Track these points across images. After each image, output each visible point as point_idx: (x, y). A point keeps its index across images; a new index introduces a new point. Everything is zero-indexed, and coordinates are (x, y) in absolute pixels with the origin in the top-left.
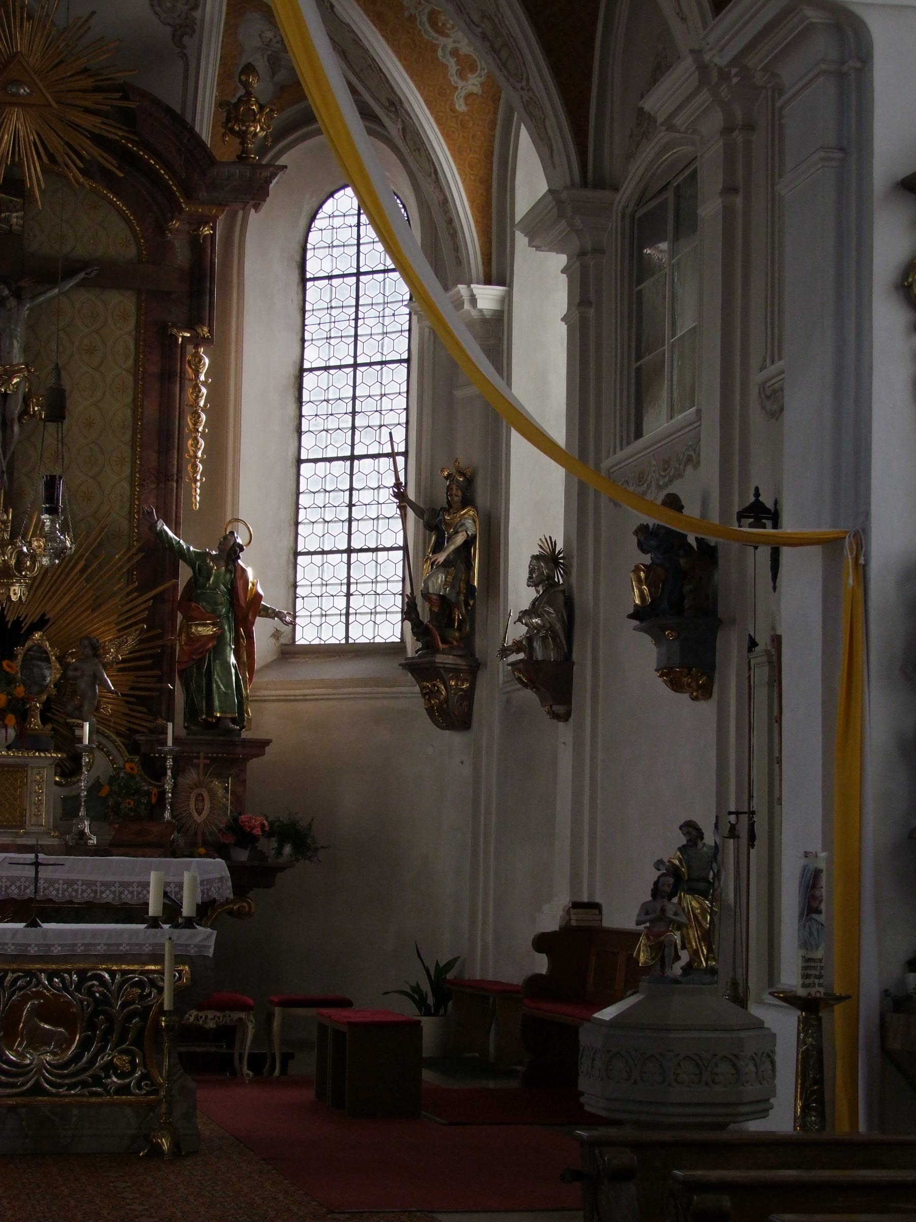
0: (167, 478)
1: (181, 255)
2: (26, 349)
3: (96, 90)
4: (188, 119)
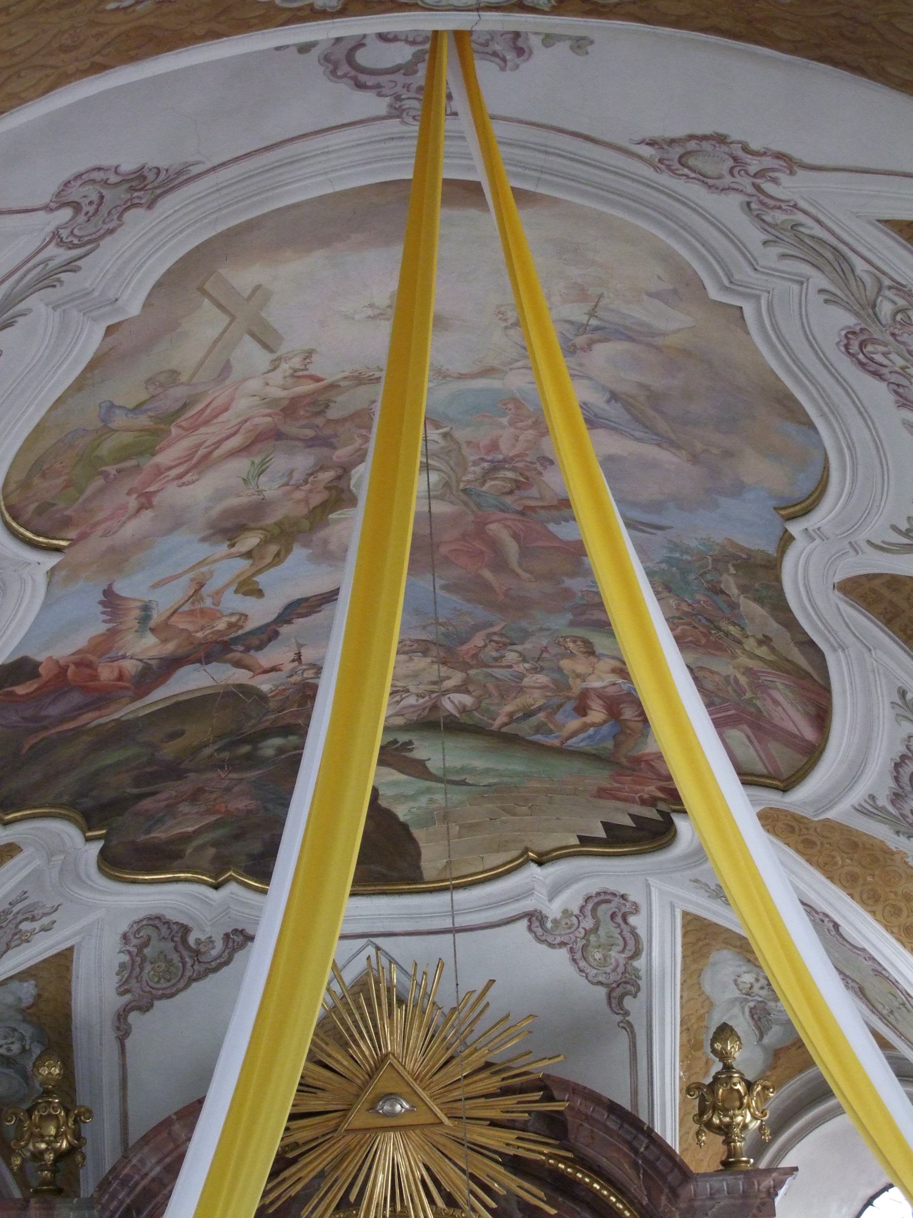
3: (506, 1091)
4: (643, 1117)
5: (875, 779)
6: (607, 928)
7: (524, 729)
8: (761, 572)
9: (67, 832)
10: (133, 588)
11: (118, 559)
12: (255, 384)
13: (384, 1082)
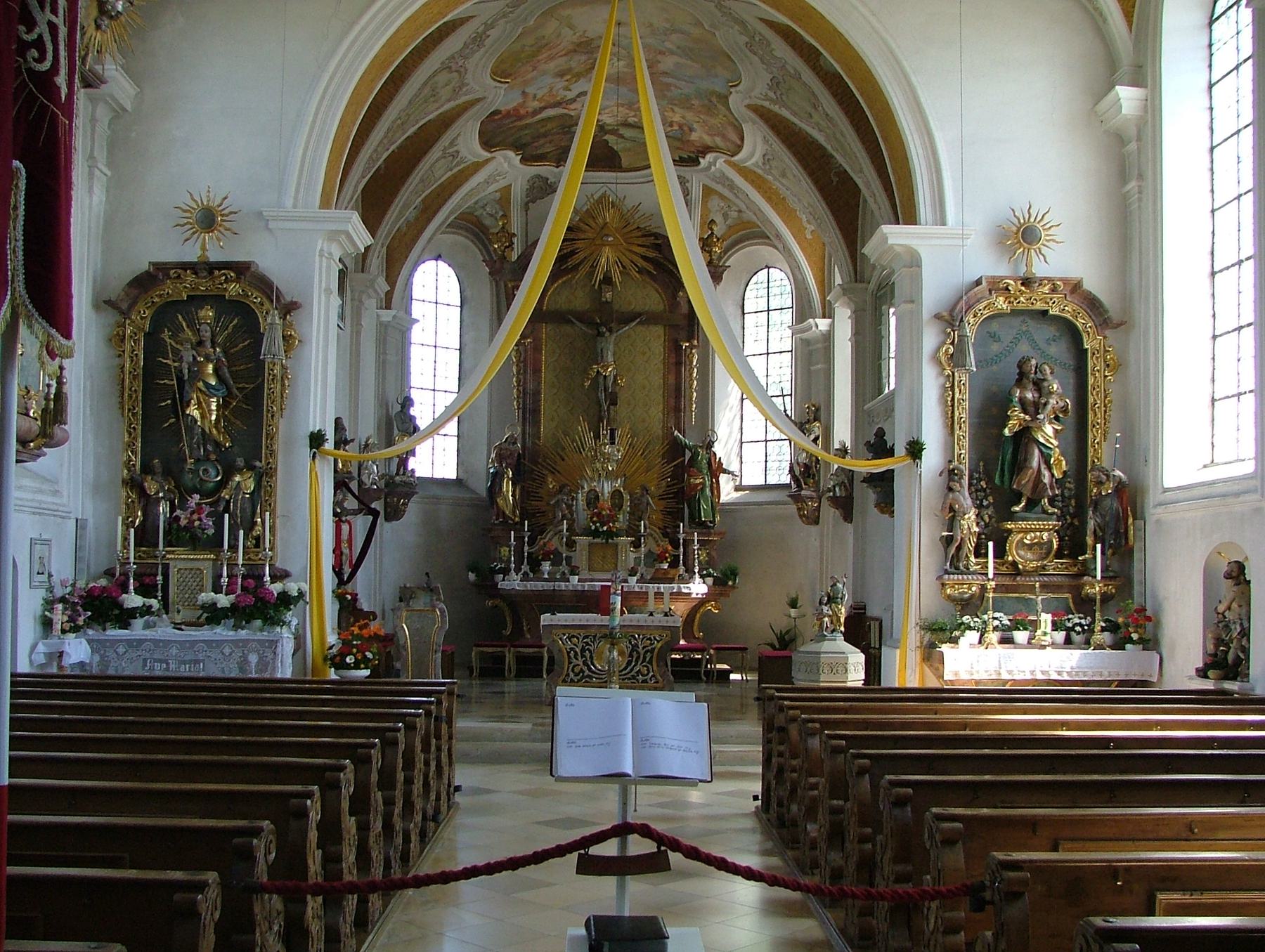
0: (680, 411)
2: (614, 354)
5: (757, 157)
8: (724, 99)
9: (511, 154)
10: (530, 90)
11: (526, 83)
12: (569, 38)
13: (605, 231)
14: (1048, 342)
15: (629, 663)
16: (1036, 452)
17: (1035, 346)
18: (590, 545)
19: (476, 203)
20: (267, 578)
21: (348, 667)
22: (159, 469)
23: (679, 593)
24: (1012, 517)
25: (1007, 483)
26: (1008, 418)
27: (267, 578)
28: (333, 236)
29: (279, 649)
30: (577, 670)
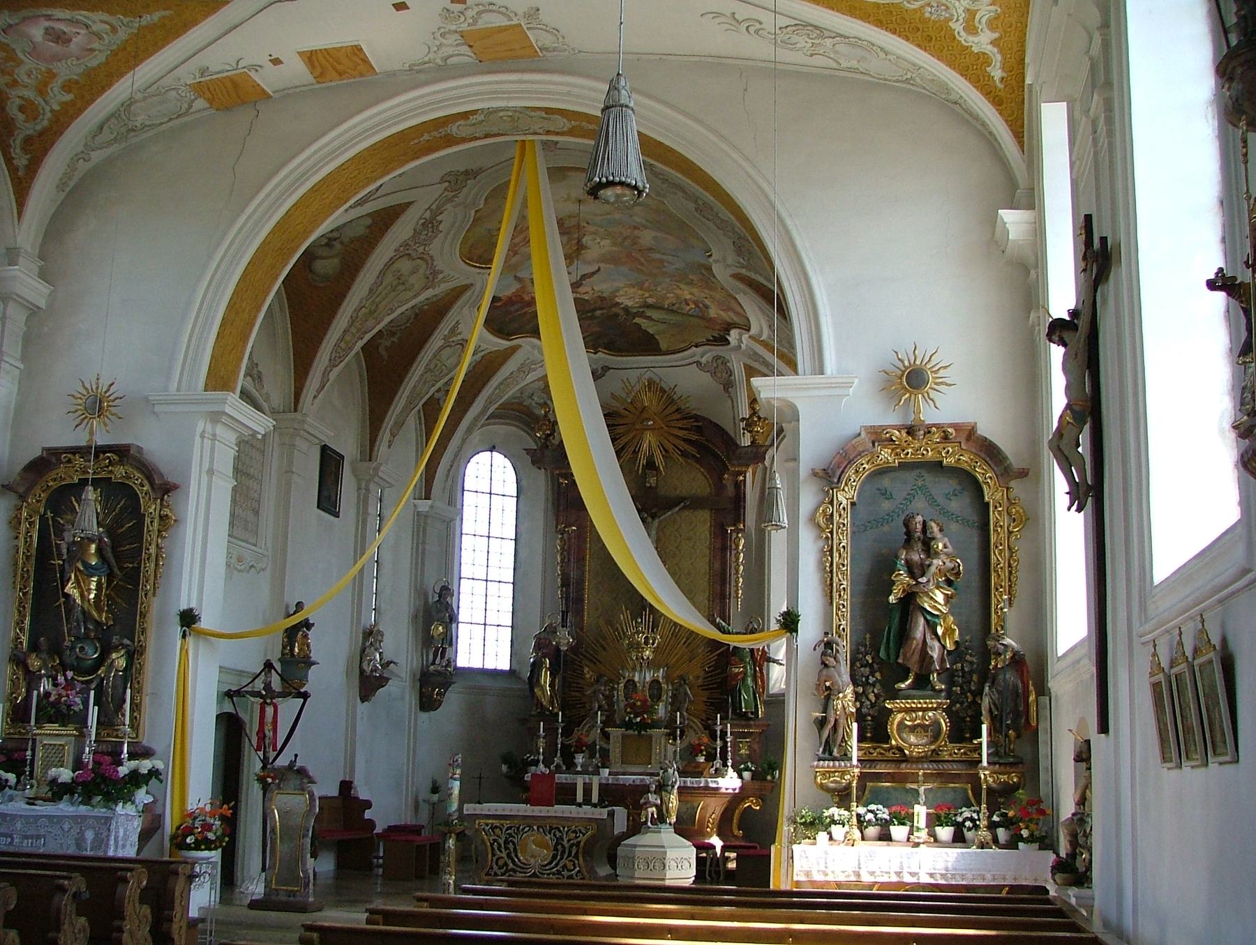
1: (730, 491)
6: (721, 367)
7: (675, 308)
13: (645, 415)
14: (948, 497)
15: (554, 857)
16: (921, 621)
17: (932, 501)
18: (624, 736)
19: (522, 391)
20: (125, 755)
21: (188, 847)
22: (44, 647)
23: (707, 788)
24: (895, 695)
25: (892, 657)
26: (893, 583)
27: (125, 755)
28: (216, 417)
29: (112, 827)
30: (501, 862)
